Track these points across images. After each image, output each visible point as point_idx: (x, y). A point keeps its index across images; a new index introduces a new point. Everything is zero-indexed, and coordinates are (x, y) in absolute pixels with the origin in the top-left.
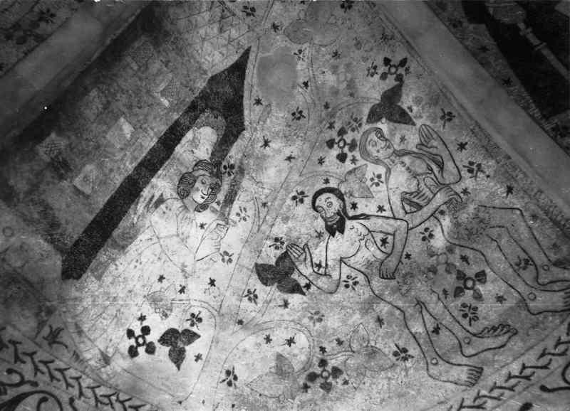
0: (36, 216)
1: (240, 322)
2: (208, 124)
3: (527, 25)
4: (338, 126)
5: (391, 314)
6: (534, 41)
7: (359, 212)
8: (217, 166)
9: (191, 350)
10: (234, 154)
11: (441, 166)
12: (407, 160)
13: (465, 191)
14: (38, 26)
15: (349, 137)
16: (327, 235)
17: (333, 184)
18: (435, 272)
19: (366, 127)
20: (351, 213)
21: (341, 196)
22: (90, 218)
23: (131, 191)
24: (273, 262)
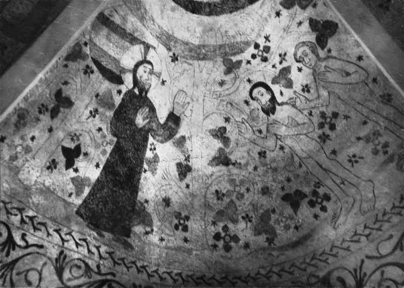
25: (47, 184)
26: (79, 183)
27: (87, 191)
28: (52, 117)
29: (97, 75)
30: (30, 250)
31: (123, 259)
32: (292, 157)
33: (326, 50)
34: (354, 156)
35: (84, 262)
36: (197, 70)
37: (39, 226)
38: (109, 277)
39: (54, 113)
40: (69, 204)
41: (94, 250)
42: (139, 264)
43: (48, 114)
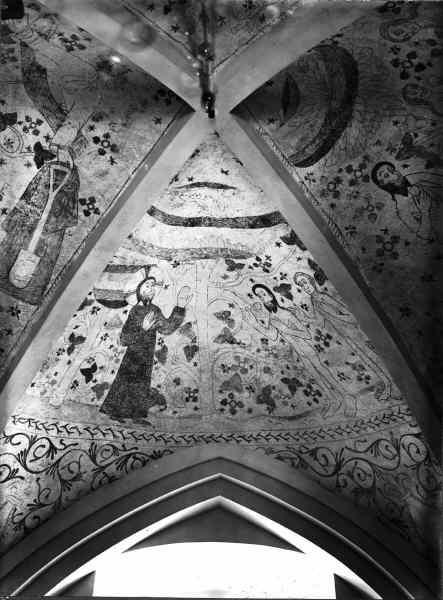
25: (72, 398)
26: (99, 389)
27: (106, 392)
28: (69, 354)
29: (104, 309)
30: (68, 449)
31: (142, 435)
32: (291, 351)
33: (323, 287)
34: (343, 374)
35: (112, 446)
36: (200, 267)
37: (72, 430)
38: (134, 451)
39: (70, 350)
40: (93, 406)
41: (118, 434)
42: (156, 435)
43: (66, 354)
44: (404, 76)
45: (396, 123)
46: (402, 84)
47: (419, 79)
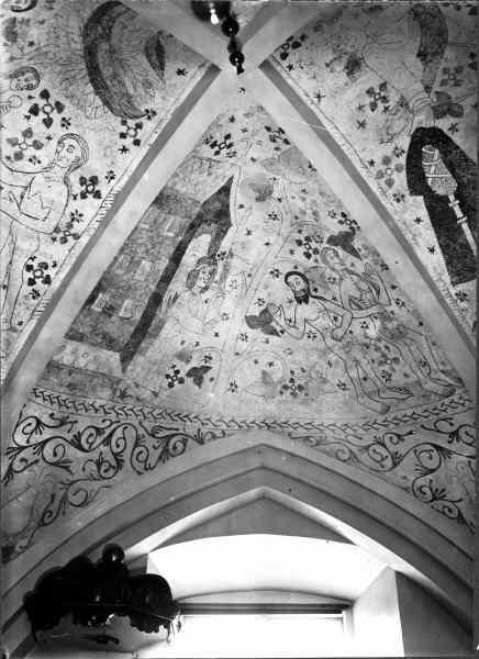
0: (100, 340)
1: (237, 354)
2: (206, 233)
3: (457, 197)
4: (305, 234)
5: (337, 362)
6: (459, 213)
7: (317, 294)
8: (212, 257)
9: (206, 377)
10: (225, 245)
11: (378, 292)
12: (354, 277)
13: (392, 312)
14: (72, 226)
15: (313, 245)
16: (295, 303)
17: (300, 270)
18: (368, 347)
19: (325, 245)
20: (314, 293)
21: (306, 280)
22: (132, 329)
23: (156, 300)
24: (257, 314)
44: (45, 95)
45: (32, 44)
46: (44, 84)
47: (30, 97)
